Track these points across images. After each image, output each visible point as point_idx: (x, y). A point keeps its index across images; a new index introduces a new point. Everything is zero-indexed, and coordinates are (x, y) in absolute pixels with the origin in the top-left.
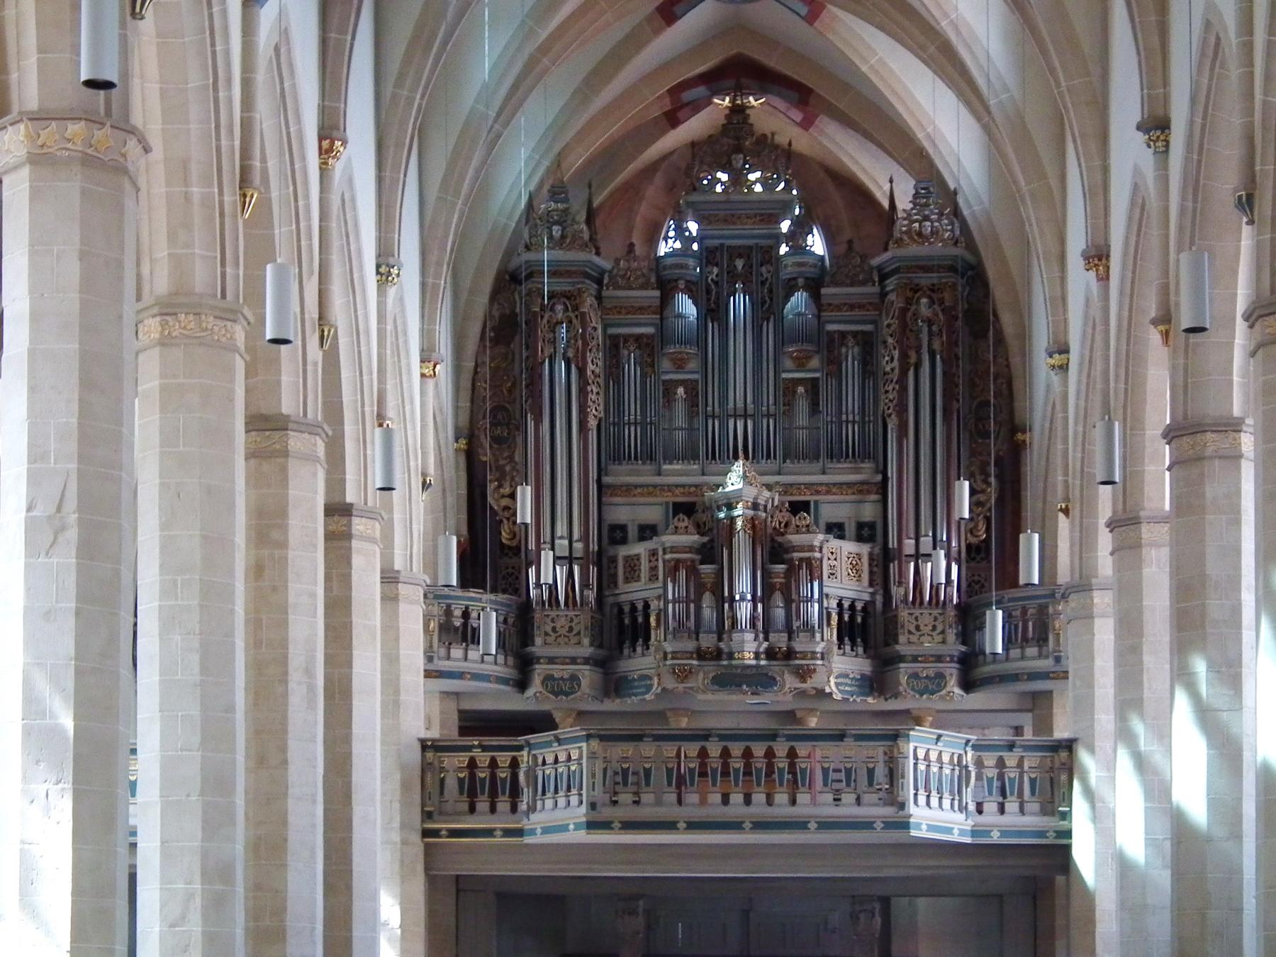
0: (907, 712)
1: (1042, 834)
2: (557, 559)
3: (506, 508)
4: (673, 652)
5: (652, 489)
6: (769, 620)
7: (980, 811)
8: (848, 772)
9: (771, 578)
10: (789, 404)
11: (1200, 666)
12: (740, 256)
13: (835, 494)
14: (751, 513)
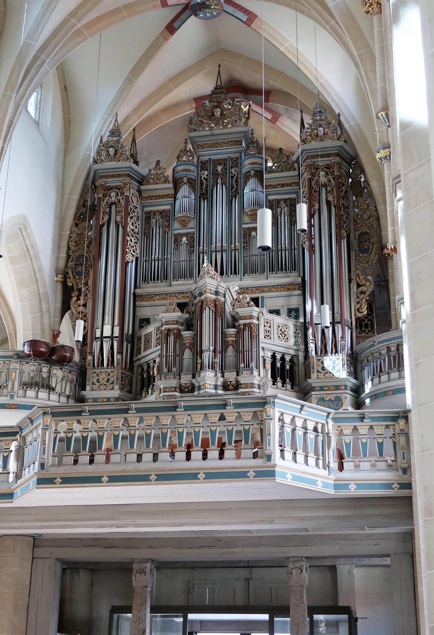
4: (164, 388)
12: (220, 164)
13: (273, 292)
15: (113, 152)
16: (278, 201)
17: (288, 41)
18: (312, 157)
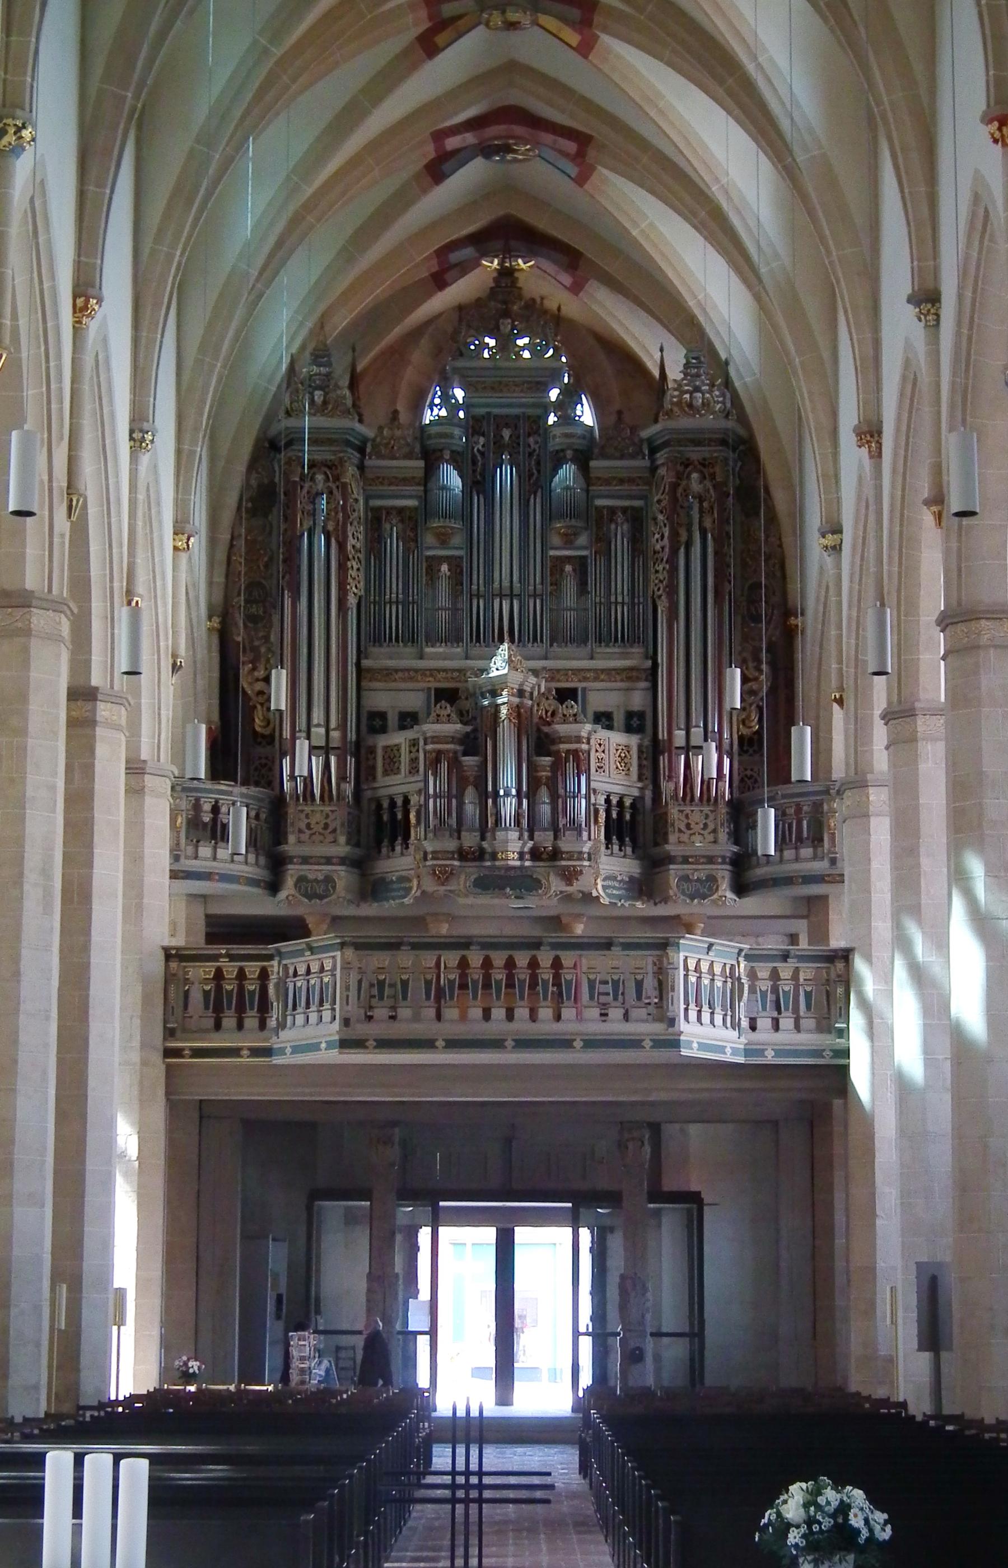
0: (677, 917)
1: (818, 1053)
2: (313, 749)
3: (261, 693)
4: (433, 852)
5: (411, 674)
6: (534, 818)
7: (753, 1028)
8: (616, 984)
9: (537, 771)
10: (555, 584)
11: (976, 867)
13: (602, 681)
14: (516, 700)
15: (322, 398)
16: (613, 511)
17: (648, 217)
18: (680, 442)
